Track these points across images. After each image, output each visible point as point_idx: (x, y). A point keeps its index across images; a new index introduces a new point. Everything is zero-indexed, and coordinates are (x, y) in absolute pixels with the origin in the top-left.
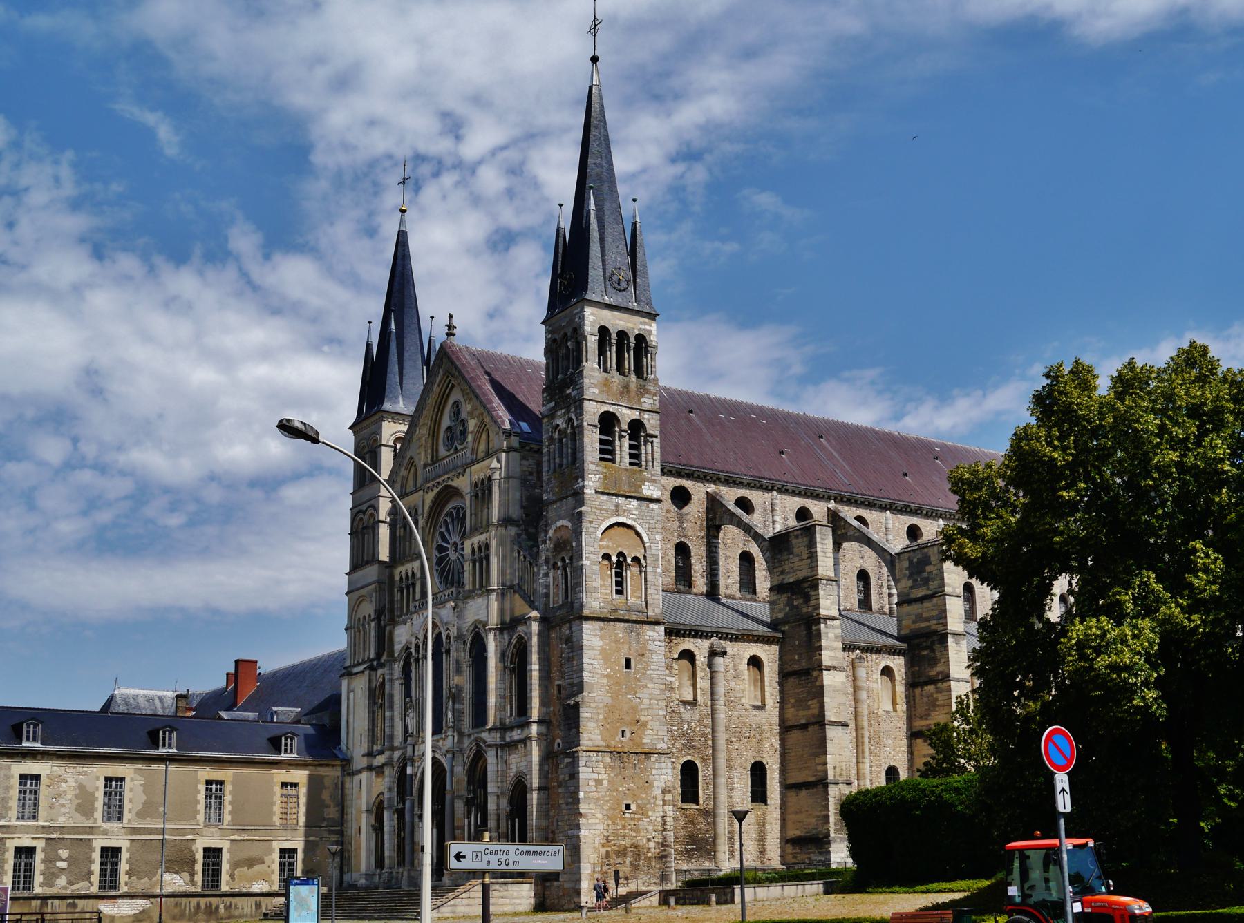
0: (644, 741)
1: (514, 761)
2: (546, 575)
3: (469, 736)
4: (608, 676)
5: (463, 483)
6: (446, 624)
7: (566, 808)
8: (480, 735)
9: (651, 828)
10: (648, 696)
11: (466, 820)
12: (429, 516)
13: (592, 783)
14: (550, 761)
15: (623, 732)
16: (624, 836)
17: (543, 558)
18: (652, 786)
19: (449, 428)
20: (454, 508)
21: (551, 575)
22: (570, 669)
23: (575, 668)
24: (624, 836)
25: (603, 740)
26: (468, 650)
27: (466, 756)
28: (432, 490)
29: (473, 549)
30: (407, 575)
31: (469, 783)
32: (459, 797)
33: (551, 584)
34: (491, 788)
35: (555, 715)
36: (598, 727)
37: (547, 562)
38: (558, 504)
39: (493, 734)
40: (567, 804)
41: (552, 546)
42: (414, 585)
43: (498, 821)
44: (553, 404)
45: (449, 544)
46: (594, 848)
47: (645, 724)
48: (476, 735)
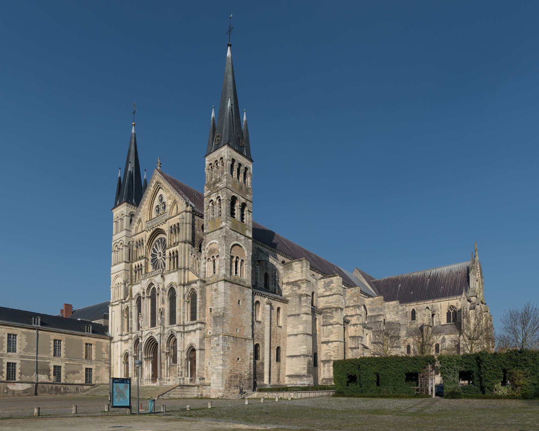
0: (244, 334)
1: (189, 338)
2: (205, 263)
3: (168, 328)
4: (232, 306)
6: (158, 283)
7: (215, 357)
8: (173, 328)
9: (246, 368)
10: (245, 316)
11: (166, 361)
12: (148, 242)
13: (226, 348)
14: (206, 339)
15: (237, 329)
16: (237, 370)
17: (204, 256)
18: (246, 351)
20: (160, 239)
21: (206, 264)
22: (217, 302)
23: (219, 302)
24: (237, 370)
25: (230, 332)
26: (167, 294)
27: (166, 336)
29: (170, 253)
30: (138, 266)
31: (167, 347)
32: (163, 352)
33: (207, 268)
34: (179, 348)
35: (208, 320)
36: (228, 326)
37: (205, 258)
39: (180, 327)
40: (215, 356)
41: (207, 252)
42: (141, 269)
43: (181, 361)
45: (157, 253)
46: (226, 374)
47: (245, 327)
48: (171, 328)
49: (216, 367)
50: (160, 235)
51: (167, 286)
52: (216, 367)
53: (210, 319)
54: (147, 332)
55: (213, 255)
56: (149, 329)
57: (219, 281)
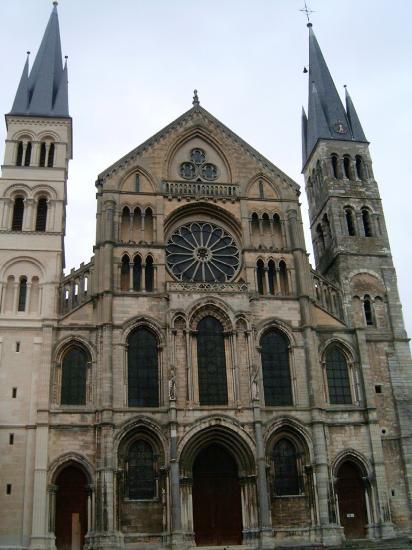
19: (187, 164)
26: (258, 338)
28: (179, 200)
30: (138, 258)
38: (361, 258)
44: (343, 192)
50: (199, 216)
51: (261, 323)
53: (382, 405)
54: (198, 414)
55: (368, 293)
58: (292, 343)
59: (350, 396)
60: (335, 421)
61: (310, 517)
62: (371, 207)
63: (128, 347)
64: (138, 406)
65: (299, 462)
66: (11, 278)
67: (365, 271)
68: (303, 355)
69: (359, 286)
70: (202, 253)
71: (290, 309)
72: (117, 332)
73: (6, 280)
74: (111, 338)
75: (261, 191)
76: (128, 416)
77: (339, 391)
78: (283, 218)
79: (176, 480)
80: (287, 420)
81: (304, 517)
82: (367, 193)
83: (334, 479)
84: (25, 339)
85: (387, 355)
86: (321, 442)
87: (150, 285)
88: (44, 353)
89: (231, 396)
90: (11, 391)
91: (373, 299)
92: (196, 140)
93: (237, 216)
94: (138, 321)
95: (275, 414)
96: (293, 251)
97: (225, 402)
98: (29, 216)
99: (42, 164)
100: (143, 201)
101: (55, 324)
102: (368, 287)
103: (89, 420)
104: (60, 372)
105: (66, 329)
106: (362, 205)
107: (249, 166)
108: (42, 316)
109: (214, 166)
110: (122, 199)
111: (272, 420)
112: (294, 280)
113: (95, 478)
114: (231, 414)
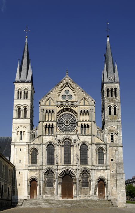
5: (77, 109)
19: (64, 95)
26: (80, 147)
28: (61, 107)
30: (49, 125)
38: (111, 122)
44: (109, 101)
49: (121, 190)
52: (121, 190)
54: (63, 167)
56: (63, 165)
57: (119, 147)
58: (89, 148)
59: (104, 162)
60: (98, 169)
61: (90, 193)
62: (117, 105)
63: (47, 150)
64: (49, 164)
65: (88, 179)
66: (18, 132)
67: (112, 126)
68: (91, 151)
69: (110, 131)
70: (67, 122)
71: (89, 138)
72: (44, 146)
73: (17, 132)
74: (43, 147)
75: (84, 103)
76: (46, 167)
77: (101, 161)
78: (89, 111)
79: (57, 183)
80: (85, 168)
81: (88, 193)
82: (116, 101)
83: (97, 184)
84: (22, 147)
85: (116, 151)
86: (94, 174)
87: (52, 133)
88: (26, 151)
89: (71, 162)
90: (19, 161)
91: (114, 134)
92: (67, 87)
93: (76, 111)
94: (49, 143)
95: (82, 167)
96: (91, 122)
97: (70, 164)
98: (22, 113)
99: (24, 98)
100: (51, 108)
101: (29, 144)
102: (113, 131)
103: (38, 168)
104: (31, 156)
105: (32, 145)
106: (114, 105)
107: (81, 95)
108: (26, 142)
109: (72, 96)
110: (45, 108)
111: (81, 168)
112: (91, 129)
113: (39, 182)
114: (71, 167)
